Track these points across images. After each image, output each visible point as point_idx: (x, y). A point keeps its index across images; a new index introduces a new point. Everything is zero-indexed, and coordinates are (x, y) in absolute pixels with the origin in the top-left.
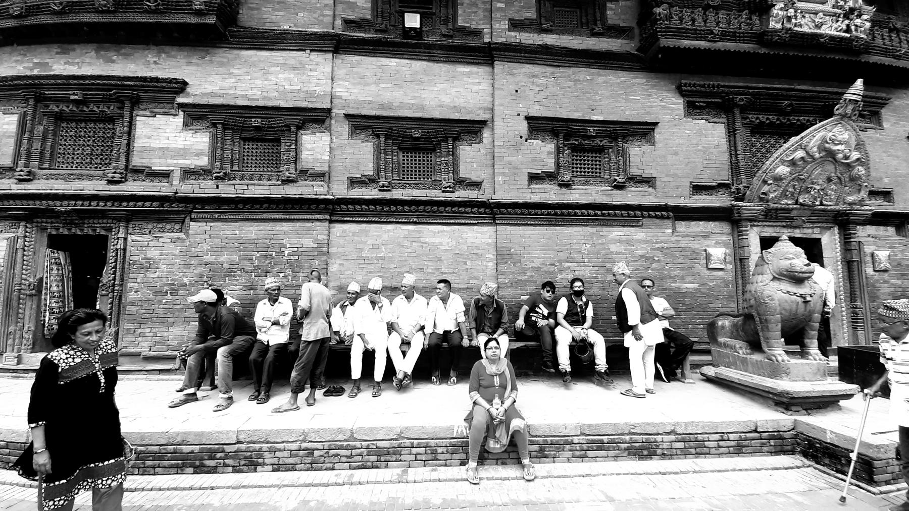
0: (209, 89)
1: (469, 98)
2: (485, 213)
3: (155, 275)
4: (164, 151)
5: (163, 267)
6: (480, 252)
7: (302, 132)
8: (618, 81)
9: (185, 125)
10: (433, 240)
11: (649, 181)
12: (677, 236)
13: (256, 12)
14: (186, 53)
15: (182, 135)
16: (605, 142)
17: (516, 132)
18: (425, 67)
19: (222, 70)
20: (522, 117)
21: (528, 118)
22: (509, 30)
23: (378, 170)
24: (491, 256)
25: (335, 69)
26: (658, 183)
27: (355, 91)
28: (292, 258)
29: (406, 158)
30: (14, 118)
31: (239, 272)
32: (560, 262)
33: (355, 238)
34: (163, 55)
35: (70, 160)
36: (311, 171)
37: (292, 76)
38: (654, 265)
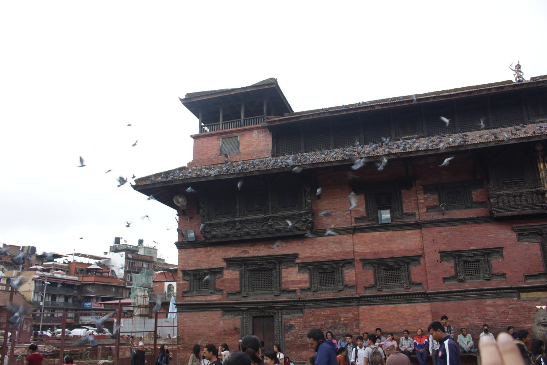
2: (425, 297)
3: (294, 331)
4: (293, 282)
5: (297, 328)
6: (424, 315)
7: (344, 269)
8: (482, 228)
9: (299, 270)
10: (402, 311)
11: (503, 275)
12: (520, 301)
13: (320, 221)
14: (296, 242)
15: (299, 275)
16: (479, 258)
17: (435, 259)
18: (391, 234)
19: (310, 247)
21: (440, 252)
22: (427, 212)
23: (376, 281)
24: (430, 316)
25: (354, 240)
26: (507, 276)
27: (363, 248)
28: (344, 322)
29: (387, 274)
30: (238, 273)
31: (324, 329)
32: (462, 317)
33: (369, 312)
34: (288, 243)
35: (257, 287)
38: (510, 316)
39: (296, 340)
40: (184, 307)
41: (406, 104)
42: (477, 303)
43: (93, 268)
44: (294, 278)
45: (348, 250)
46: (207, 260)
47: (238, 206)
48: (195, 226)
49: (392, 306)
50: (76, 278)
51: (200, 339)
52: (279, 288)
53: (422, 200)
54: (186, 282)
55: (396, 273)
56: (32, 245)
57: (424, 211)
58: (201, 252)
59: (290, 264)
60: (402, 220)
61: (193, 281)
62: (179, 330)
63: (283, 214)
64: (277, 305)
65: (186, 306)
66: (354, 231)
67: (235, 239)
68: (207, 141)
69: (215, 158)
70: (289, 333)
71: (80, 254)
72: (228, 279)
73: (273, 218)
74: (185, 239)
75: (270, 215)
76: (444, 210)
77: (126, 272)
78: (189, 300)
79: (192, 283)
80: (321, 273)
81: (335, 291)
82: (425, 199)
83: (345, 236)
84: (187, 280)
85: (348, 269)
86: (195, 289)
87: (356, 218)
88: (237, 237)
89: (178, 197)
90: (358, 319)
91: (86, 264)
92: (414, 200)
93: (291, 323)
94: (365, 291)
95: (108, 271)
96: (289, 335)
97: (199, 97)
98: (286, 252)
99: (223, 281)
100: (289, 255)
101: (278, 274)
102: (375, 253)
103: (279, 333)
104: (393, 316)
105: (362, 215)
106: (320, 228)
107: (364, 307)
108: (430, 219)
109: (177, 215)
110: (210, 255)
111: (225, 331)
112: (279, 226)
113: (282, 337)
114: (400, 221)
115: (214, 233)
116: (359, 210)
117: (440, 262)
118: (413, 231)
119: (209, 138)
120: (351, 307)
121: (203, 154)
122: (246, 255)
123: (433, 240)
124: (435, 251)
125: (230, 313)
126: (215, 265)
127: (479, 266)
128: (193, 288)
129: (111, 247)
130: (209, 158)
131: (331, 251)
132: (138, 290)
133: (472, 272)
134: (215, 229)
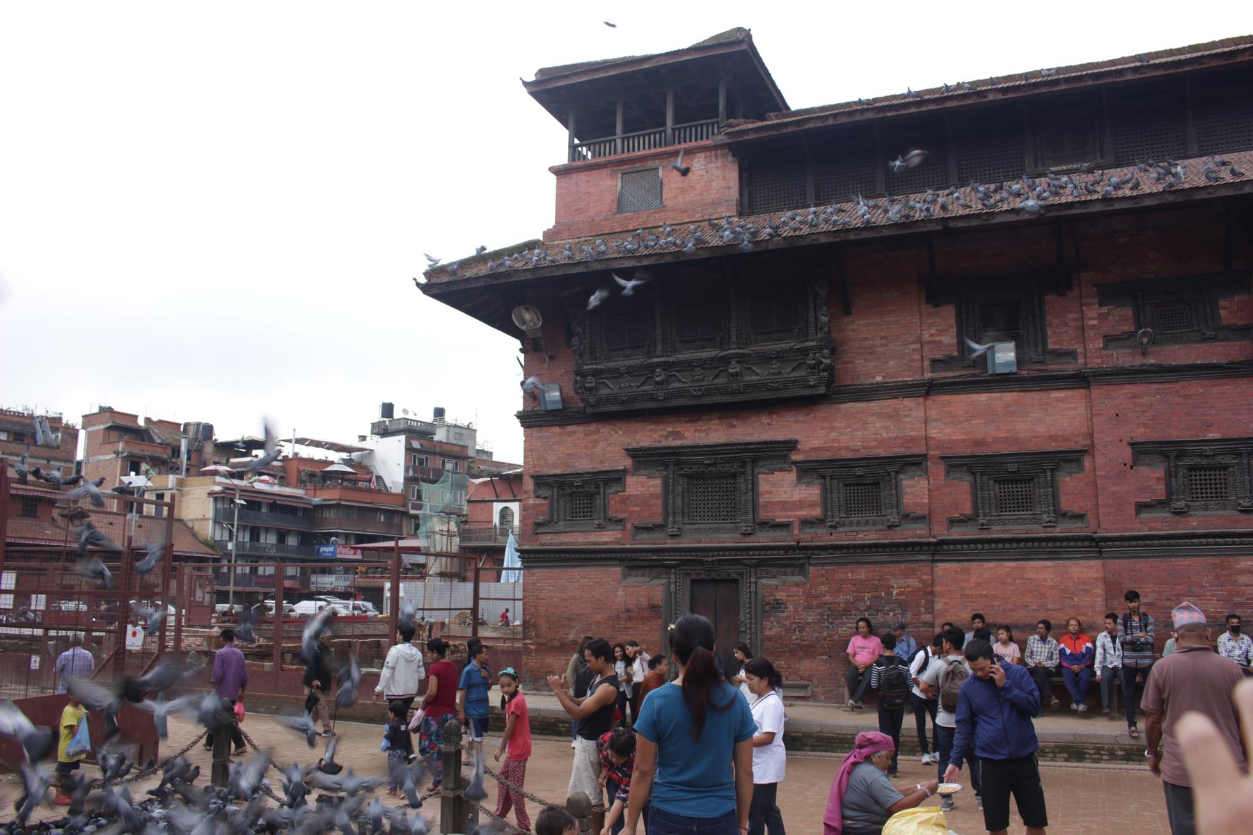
0: (816, 443)
1: (1066, 425)
2: (1090, 547)
3: (784, 615)
4: (784, 505)
5: (791, 607)
6: (1087, 587)
7: (902, 476)
8: (1239, 390)
9: (799, 478)
10: (1036, 576)
13: (850, 365)
14: (793, 413)
15: (797, 488)
16: (1227, 460)
17: (1120, 460)
18: (1016, 397)
19: (826, 424)
20: (1124, 443)
21: (1132, 444)
22: (1106, 347)
24: (1100, 591)
25: (928, 410)
27: (948, 430)
28: (900, 597)
29: (1002, 490)
30: (659, 482)
31: (853, 612)
33: (958, 576)
34: (774, 416)
35: (702, 514)
36: (912, 515)
37: (889, 424)
39: (790, 634)
40: (537, 555)
41: (1063, 87)
42: (1216, 564)
43: (337, 472)
44: (785, 496)
45: (913, 433)
46: (589, 453)
47: (659, 331)
48: (561, 375)
49: (1012, 564)
50: (299, 492)
51: (574, 627)
52: (751, 517)
53: (1093, 319)
54: (543, 502)
55: (1024, 489)
56: (204, 421)
57: (1097, 346)
58: (577, 435)
59: (778, 463)
60: (1044, 367)
61: (558, 499)
62: (527, 607)
63: (764, 348)
64: (748, 555)
65: (542, 555)
66: (929, 389)
67: (653, 405)
68: (588, 181)
69: (606, 219)
70: (772, 619)
71: (307, 440)
72: (637, 496)
73: (741, 359)
74: (540, 405)
75: (734, 351)
76: (1148, 343)
77: (408, 481)
78: (548, 540)
79: (555, 504)
80: (850, 485)
81: (879, 527)
82: (1101, 317)
83: (908, 402)
84: (545, 498)
85: (913, 478)
86: (562, 516)
87: (934, 361)
88: (658, 400)
89: (523, 311)
90: (932, 593)
91: (320, 461)
92: (1075, 320)
93: (778, 598)
94: (949, 529)
95: (368, 477)
96: (772, 622)
97: (566, 77)
98: (768, 436)
99: (624, 501)
100: (776, 442)
101: (750, 486)
102: (976, 443)
103: (750, 618)
104: (1012, 588)
105: (947, 353)
106: (849, 382)
107: (947, 565)
108: (1110, 364)
109: (521, 350)
110: (597, 441)
111: (628, 610)
112: (755, 378)
113: (756, 628)
114: (1039, 368)
115: (604, 392)
116: (940, 342)
117: (1131, 467)
118: (1070, 393)
119: (591, 172)
120: (916, 565)
121: (578, 210)
122: (678, 443)
123: (1117, 415)
124: (1121, 440)
125: (639, 572)
126: (606, 465)
127: (1225, 479)
128: (558, 515)
129: (373, 424)
130: (593, 220)
131: (874, 436)
132: (435, 519)
133: (1207, 493)
134: (608, 382)
